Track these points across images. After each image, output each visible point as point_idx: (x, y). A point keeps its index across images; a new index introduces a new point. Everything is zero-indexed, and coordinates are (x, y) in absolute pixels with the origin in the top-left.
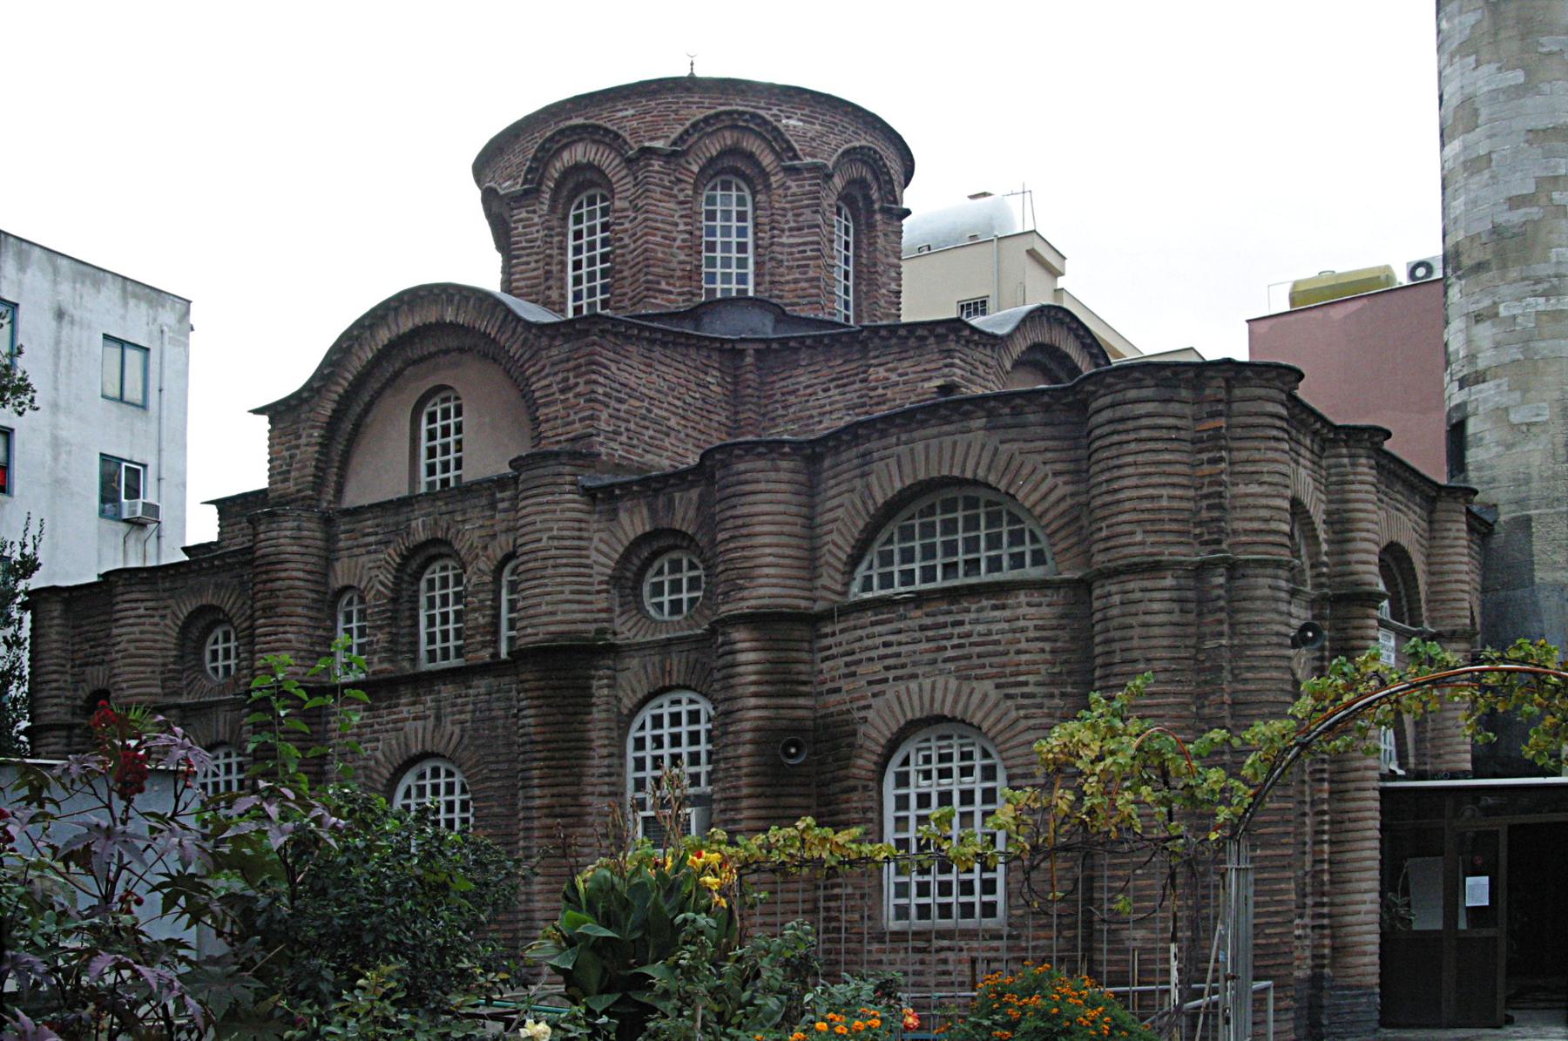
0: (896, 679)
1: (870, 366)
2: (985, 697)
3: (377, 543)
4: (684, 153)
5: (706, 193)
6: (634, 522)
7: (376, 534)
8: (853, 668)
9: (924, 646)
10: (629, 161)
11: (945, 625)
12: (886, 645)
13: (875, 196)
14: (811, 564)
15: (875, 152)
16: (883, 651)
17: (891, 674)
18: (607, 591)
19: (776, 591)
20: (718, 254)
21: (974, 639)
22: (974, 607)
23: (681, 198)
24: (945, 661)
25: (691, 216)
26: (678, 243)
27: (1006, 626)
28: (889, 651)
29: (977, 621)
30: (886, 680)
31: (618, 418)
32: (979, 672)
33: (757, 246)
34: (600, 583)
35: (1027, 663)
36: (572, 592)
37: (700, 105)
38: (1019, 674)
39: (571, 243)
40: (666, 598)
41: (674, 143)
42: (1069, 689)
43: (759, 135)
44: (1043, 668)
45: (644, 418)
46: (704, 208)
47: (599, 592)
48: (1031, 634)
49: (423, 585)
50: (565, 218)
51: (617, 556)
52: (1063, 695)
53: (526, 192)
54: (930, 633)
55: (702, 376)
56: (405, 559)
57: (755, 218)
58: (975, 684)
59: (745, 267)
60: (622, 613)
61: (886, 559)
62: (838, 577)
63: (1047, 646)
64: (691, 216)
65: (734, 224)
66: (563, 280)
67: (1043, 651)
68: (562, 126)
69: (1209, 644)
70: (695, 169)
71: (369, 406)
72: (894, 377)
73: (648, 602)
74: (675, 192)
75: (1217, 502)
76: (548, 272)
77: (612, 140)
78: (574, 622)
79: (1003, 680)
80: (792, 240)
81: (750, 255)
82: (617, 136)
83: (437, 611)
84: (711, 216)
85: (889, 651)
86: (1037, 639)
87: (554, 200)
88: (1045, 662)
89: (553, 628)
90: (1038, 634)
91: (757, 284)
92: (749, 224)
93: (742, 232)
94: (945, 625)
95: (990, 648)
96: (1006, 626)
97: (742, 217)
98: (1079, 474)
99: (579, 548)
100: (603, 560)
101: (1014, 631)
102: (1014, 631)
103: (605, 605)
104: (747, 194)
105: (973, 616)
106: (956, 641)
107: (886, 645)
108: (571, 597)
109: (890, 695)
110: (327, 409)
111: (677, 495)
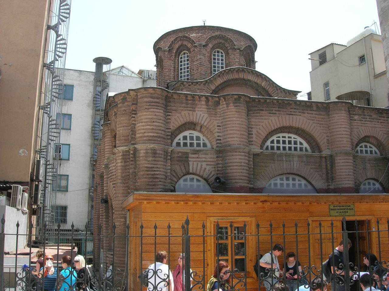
4: (173, 48)
15: (222, 35)
26: (172, 70)
41: (169, 48)
70: (175, 52)
80: (197, 63)
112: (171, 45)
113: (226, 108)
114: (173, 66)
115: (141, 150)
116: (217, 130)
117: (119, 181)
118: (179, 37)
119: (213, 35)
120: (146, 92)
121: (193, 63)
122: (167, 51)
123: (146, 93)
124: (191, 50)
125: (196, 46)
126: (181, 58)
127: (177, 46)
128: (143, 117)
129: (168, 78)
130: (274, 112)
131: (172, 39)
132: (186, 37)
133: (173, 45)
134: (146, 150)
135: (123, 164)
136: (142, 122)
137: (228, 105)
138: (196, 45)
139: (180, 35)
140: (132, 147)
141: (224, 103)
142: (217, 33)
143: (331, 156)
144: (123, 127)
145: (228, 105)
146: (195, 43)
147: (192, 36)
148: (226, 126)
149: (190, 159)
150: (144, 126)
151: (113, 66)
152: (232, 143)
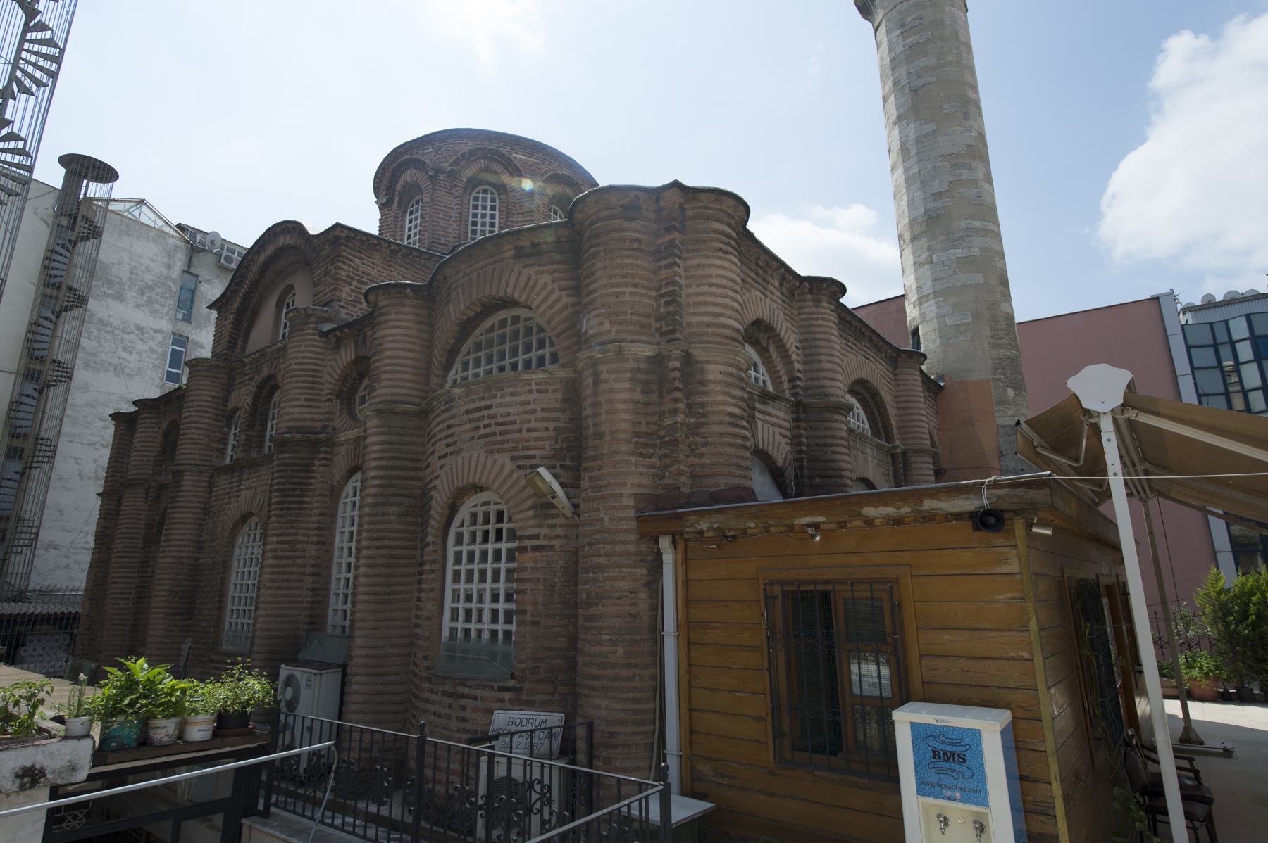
0: (452, 453)
6: (347, 355)
9: (468, 426)
11: (479, 409)
12: (449, 427)
17: (450, 449)
18: (330, 400)
19: (396, 390)
20: (479, 228)
21: (500, 419)
22: (499, 394)
24: (480, 437)
27: (521, 409)
29: (501, 405)
30: (445, 456)
35: (537, 439)
38: (528, 449)
39: (407, 226)
42: (568, 462)
43: (499, 163)
44: (547, 443)
48: (539, 415)
50: (405, 213)
52: (562, 467)
54: (471, 416)
56: (260, 388)
58: (497, 456)
63: (552, 425)
65: (488, 212)
67: (547, 429)
69: (668, 422)
73: (358, 408)
78: (306, 420)
79: (517, 454)
84: (475, 207)
86: (541, 420)
87: (400, 202)
88: (549, 439)
89: (291, 424)
90: (546, 415)
92: (497, 213)
93: (493, 216)
94: (479, 409)
95: (509, 427)
96: (521, 409)
97: (493, 208)
98: (577, 288)
99: (315, 371)
100: (330, 379)
101: (526, 412)
102: (526, 412)
104: (496, 195)
105: (498, 401)
106: (486, 421)
109: (448, 467)
110: (236, 305)
112: (456, 163)
118: (483, 149)
120: (718, 206)
122: (443, 172)
123: (717, 209)
126: (476, 199)
128: (713, 271)
132: (502, 155)
135: (638, 396)
136: (711, 285)
139: (487, 145)
141: (809, 297)
144: (635, 286)
148: (815, 351)
149: (757, 415)
151: (119, 189)
152: (832, 391)
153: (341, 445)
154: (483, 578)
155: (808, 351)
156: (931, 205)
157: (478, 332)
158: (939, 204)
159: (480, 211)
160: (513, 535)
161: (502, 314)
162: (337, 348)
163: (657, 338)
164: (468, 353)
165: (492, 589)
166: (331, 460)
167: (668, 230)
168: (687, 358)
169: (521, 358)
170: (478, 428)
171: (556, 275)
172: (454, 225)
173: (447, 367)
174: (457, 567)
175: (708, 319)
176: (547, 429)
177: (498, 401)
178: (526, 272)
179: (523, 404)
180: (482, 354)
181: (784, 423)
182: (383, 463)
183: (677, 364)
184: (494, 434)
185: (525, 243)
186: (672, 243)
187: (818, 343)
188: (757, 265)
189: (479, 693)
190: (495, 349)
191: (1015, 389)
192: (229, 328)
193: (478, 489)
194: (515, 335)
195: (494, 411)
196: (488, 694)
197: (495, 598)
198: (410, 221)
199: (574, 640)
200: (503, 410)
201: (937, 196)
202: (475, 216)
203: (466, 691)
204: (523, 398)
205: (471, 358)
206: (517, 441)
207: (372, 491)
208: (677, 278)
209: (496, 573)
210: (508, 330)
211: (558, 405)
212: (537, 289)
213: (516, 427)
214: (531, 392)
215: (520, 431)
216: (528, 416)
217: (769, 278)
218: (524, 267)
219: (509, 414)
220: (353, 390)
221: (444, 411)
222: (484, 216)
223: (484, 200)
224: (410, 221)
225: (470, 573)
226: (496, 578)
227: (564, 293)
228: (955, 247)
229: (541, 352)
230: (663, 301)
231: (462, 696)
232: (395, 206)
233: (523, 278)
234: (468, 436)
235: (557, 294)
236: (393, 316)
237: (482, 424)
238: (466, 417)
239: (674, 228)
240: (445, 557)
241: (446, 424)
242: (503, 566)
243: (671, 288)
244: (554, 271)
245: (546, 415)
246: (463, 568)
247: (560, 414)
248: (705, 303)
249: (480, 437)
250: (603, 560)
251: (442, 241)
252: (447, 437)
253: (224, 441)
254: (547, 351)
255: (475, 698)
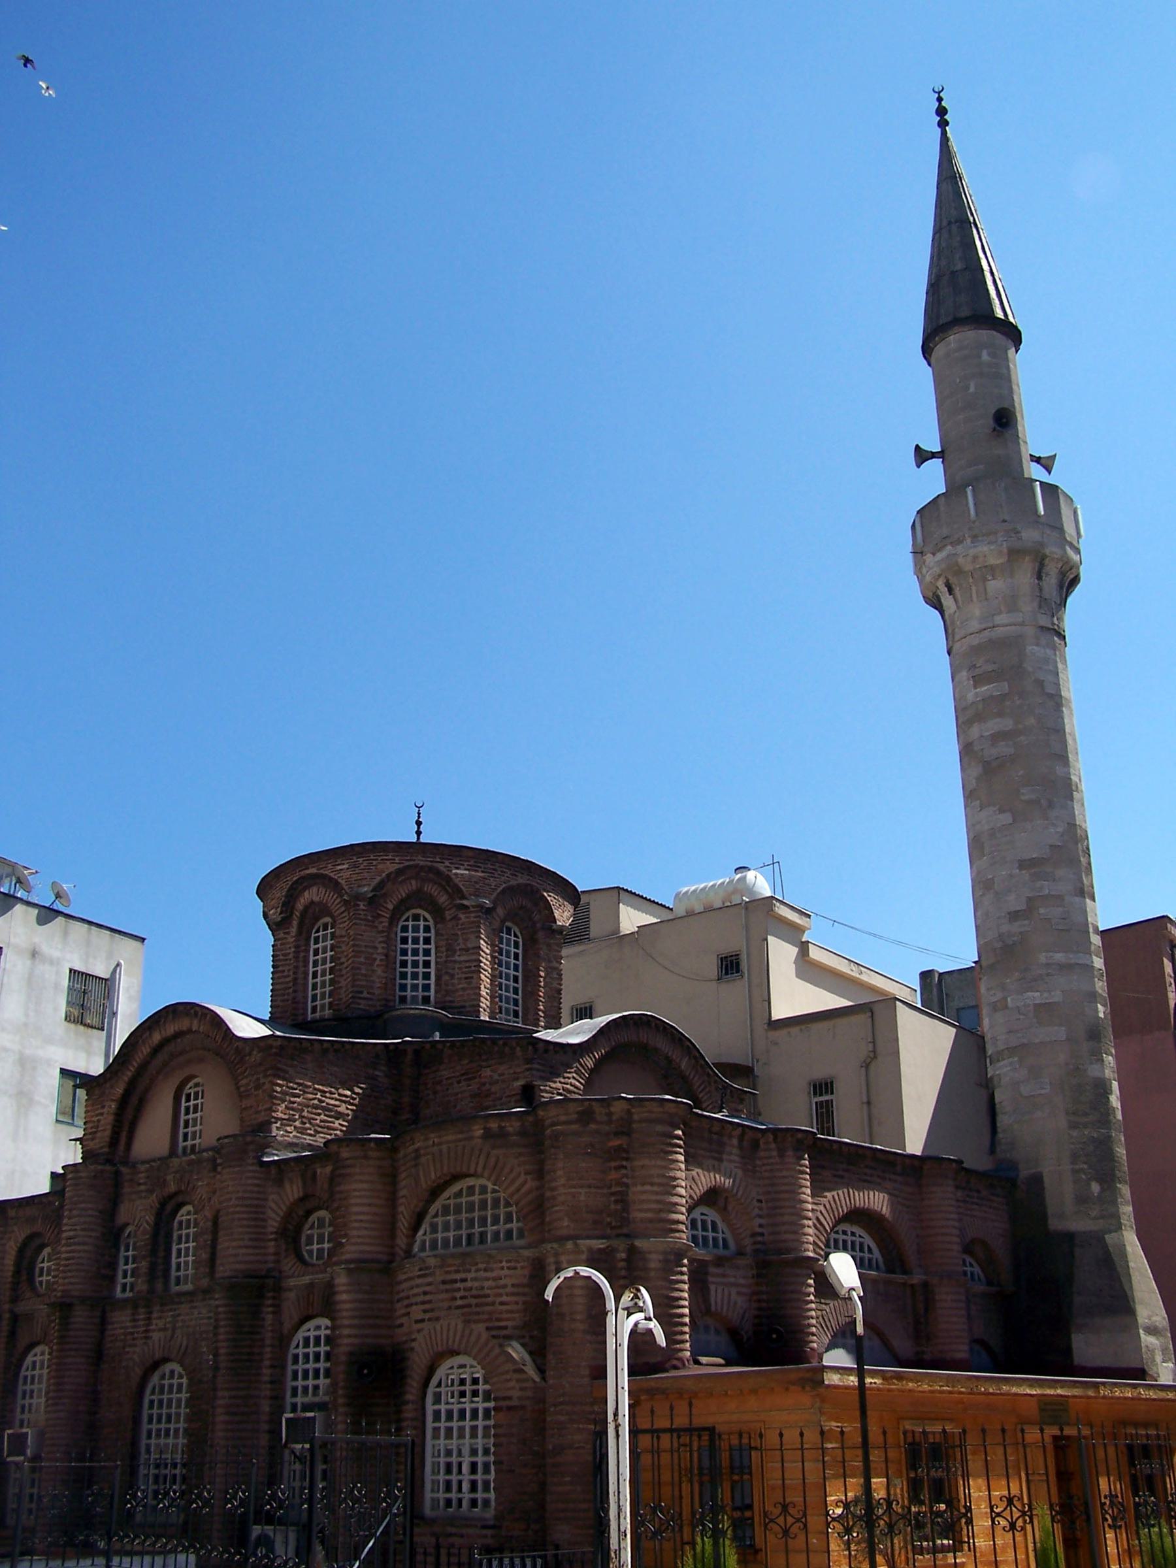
0: (429, 1320)
1: (481, 1067)
2: (479, 1336)
3: (147, 1191)
5: (401, 923)
6: (293, 1190)
7: (145, 1184)
8: (408, 1310)
10: (346, 902)
11: (455, 1281)
12: (425, 1293)
13: (537, 918)
14: (390, 1228)
16: (422, 1298)
17: (427, 1316)
18: (275, 1240)
21: (474, 1292)
22: (473, 1269)
23: (380, 928)
25: (388, 941)
26: (377, 962)
28: (428, 1298)
30: (423, 1321)
31: (293, 1109)
32: (476, 1317)
33: (437, 963)
34: (272, 1233)
36: (251, 1239)
37: (392, 861)
38: (498, 1320)
39: (312, 958)
40: (315, 1247)
45: (316, 1108)
46: (400, 934)
47: (270, 1240)
48: (509, 1289)
49: (176, 1224)
51: (282, 1214)
53: (283, 919)
54: (448, 1287)
55: (371, 1071)
56: (163, 1205)
57: (436, 943)
58: (473, 1326)
59: (429, 979)
60: (286, 1257)
61: (434, 1229)
62: (405, 1240)
63: (521, 1299)
64: (388, 941)
65: (421, 946)
66: (306, 985)
67: (517, 1303)
68: (302, 873)
70: (391, 907)
71: (147, 1090)
72: (496, 1077)
74: (376, 924)
75: (623, 1200)
76: (295, 979)
77: (333, 884)
79: (491, 1325)
80: (462, 958)
81: (433, 970)
82: (337, 883)
83: (182, 1246)
85: (428, 1298)
86: (513, 1294)
90: (515, 1290)
91: (436, 992)
92: (432, 947)
94: (455, 1281)
95: (483, 1300)
97: (427, 941)
99: (257, 1206)
100: (273, 1215)
101: (497, 1287)
102: (497, 1287)
103: (272, 1250)
104: (431, 923)
105: (472, 1275)
106: (462, 1293)
107: (425, 1293)
108: (250, 1243)
110: (119, 1090)
111: (319, 1171)
113: (777, 1159)
114: (380, 950)
115: (650, 1253)
116: (756, 1211)
117: (581, 1326)
118: (416, 866)
119: (513, 883)
121: (453, 955)
122: (364, 900)
124: (448, 915)
125: (466, 907)
126: (405, 929)
127: (403, 892)
129: (364, 983)
130: (840, 1173)
131: (393, 867)
132: (438, 873)
133: (389, 885)
134: (665, 1253)
136: (652, 1184)
137: (782, 1153)
138: (465, 902)
139: (420, 861)
140: (621, 1245)
141: (773, 1146)
142: (522, 879)
143: (925, 1285)
144: (590, 1187)
145: (782, 1153)
146: (463, 897)
147: (456, 874)
149: (710, 1279)
150: (657, 1193)
153: (290, 1290)
154: (461, 1436)
155: (770, 1204)
156: (1005, 928)
157: (446, 1194)
158: (1016, 927)
159: (410, 946)
160: (487, 1397)
161: (471, 1181)
162: (279, 1182)
163: (609, 1231)
164: (436, 1215)
165: (471, 1445)
166: (278, 1306)
167: (617, 1134)
168: (632, 1251)
169: (491, 1229)
170: (455, 1299)
171: (522, 1159)
172: (379, 971)
173: (415, 1228)
174: (436, 1425)
175: (649, 1215)
176: (517, 1303)
177: (472, 1275)
178: (495, 1152)
179: (494, 1279)
180: (451, 1218)
181: (742, 1281)
182: (356, 1322)
183: (623, 1255)
184: (470, 1306)
185: (494, 1125)
186: (619, 1149)
187: (782, 1196)
188: (710, 1132)
189: (464, 1531)
190: (464, 1215)
191: (1101, 1181)
192: (107, 1120)
193: (454, 1353)
194: (483, 1204)
195: (469, 1284)
196: (471, 1531)
197: (474, 1452)
198: (316, 952)
199: (543, 1485)
200: (476, 1284)
201: (1014, 916)
202: (404, 952)
203: (454, 1530)
204: (494, 1274)
205: (439, 1220)
206: (490, 1313)
207: (343, 1349)
208: (625, 1180)
209: (474, 1429)
210: (476, 1198)
211: (525, 1281)
212: (506, 1170)
213: (490, 1300)
214: (502, 1268)
215: (493, 1304)
216: (501, 1291)
217: (725, 1139)
218: (494, 1147)
219: (482, 1288)
220: (299, 1230)
221: (419, 1277)
222: (415, 952)
223: (416, 929)
224: (316, 952)
225: (449, 1430)
226: (474, 1435)
227: (529, 1177)
228: (1031, 989)
229: (508, 1226)
230: (613, 1199)
231: (451, 1535)
232: (294, 930)
233: (492, 1160)
234: (446, 1304)
235: (522, 1178)
236: (357, 1170)
237: (458, 1295)
238: (442, 1287)
239: (623, 1133)
240: (424, 1415)
241: (421, 1290)
242: (480, 1423)
243: (619, 1189)
244: (520, 1154)
245: (515, 1290)
246: (443, 1425)
247: (526, 1290)
248: (648, 1201)
249: (458, 1307)
250: (562, 1418)
251: (365, 995)
252: (423, 1303)
253: (113, 1265)
254: (514, 1225)
255: (462, 1536)
